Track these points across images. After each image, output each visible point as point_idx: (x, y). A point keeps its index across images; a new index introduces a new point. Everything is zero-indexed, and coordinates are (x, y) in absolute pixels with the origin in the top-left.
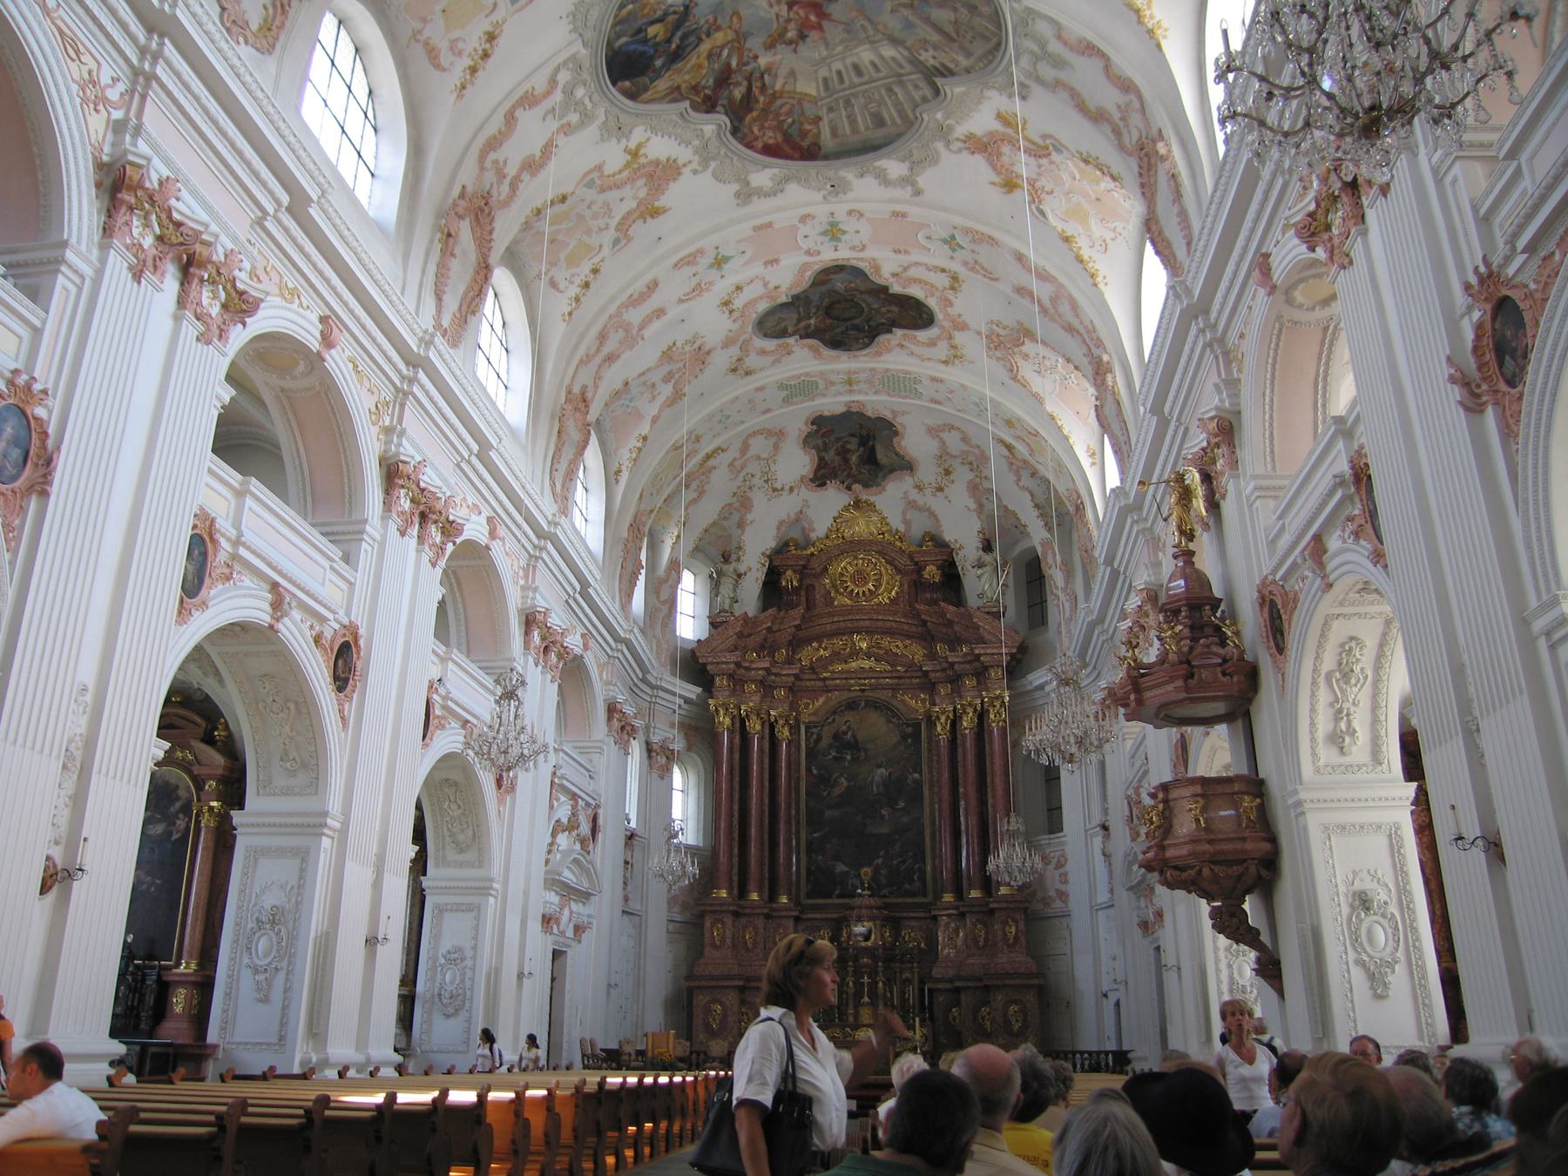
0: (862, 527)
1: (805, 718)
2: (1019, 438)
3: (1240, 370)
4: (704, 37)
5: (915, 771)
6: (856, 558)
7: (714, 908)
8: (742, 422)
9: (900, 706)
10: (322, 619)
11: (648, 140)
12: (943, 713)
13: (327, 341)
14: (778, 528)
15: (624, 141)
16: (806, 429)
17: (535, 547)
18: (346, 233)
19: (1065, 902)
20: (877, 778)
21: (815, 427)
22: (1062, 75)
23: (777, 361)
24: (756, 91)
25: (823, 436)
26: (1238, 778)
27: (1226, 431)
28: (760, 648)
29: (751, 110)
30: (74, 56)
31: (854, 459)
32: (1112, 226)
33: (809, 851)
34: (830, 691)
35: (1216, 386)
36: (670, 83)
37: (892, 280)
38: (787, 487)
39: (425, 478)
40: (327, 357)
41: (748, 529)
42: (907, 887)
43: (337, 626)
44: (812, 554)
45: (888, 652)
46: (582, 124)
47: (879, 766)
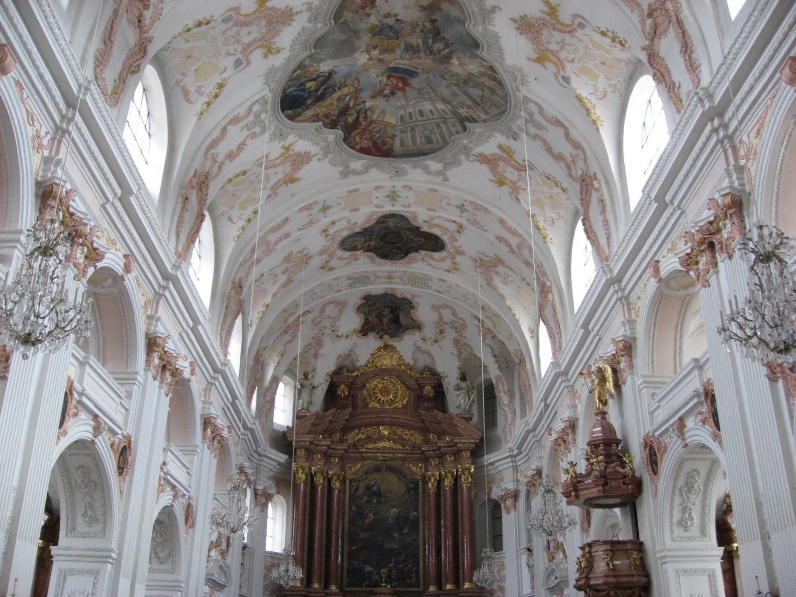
0: (387, 362)
1: (349, 476)
2: (487, 317)
3: (637, 316)
4: (337, 89)
5: (415, 511)
6: (383, 379)
7: (292, 593)
8: (323, 297)
9: (407, 471)
10: (114, 433)
11: (296, 142)
12: (433, 476)
13: (127, 269)
14: (338, 359)
15: (282, 142)
16: (360, 302)
17: (212, 377)
18: (146, 209)
19: (503, 593)
20: (392, 514)
21: (365, 301)
22: (540, 133)
23: (349, 263)
24: (361, 119)
25: (369, 306)
26: (630, 541)
27: (628, 348)
28: (324, 432)
29: (357, 129)
30: (31, 123)
31: (386, 320)
32: (558, 211)
33: (349, 559)
34: (364, 460)
35: (623, 323)
36: (313, 113)
37: (423, 224)
38: (345, 335)
39: (167, 345)
40: (126, 278)
41: (320, 360)
42: (408, 581)
43: (120, 437)
44: (357, 376)
45: (401, 437)
46: (262, 133)
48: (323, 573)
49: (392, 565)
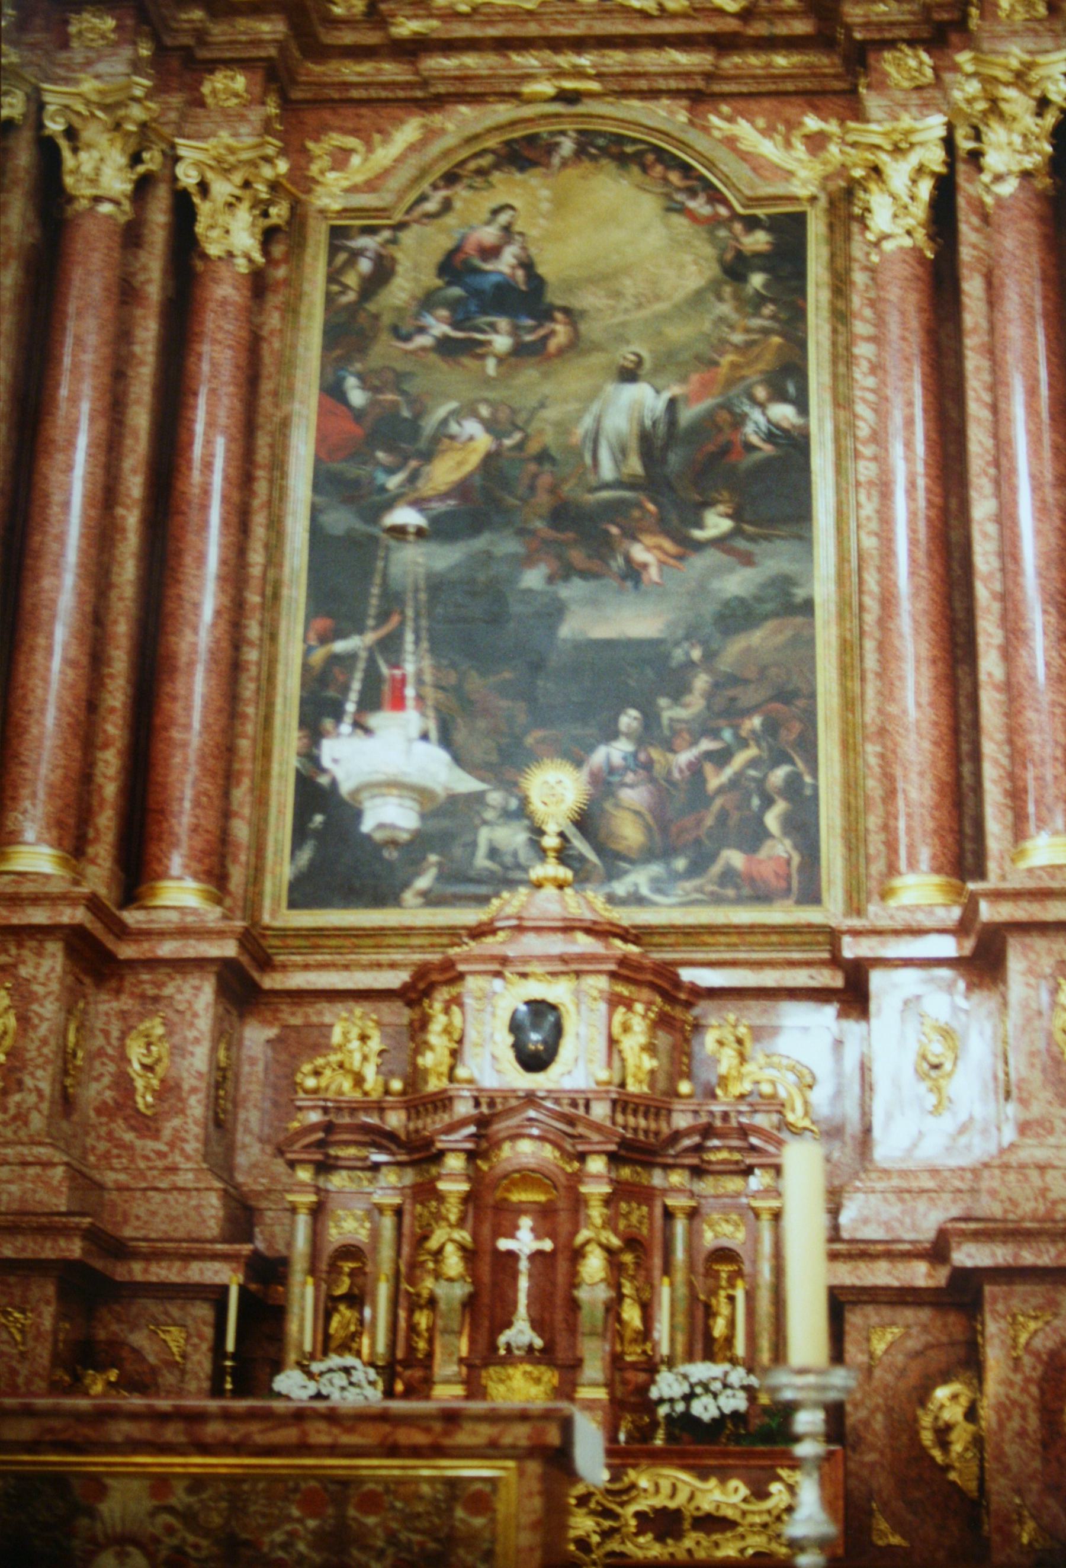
5: (779, 395)
12: (898, 151)
34: (437, 102)
42: (735, 858)
47: (629, 375)
48: (110, 790)
49: (618, 751)
